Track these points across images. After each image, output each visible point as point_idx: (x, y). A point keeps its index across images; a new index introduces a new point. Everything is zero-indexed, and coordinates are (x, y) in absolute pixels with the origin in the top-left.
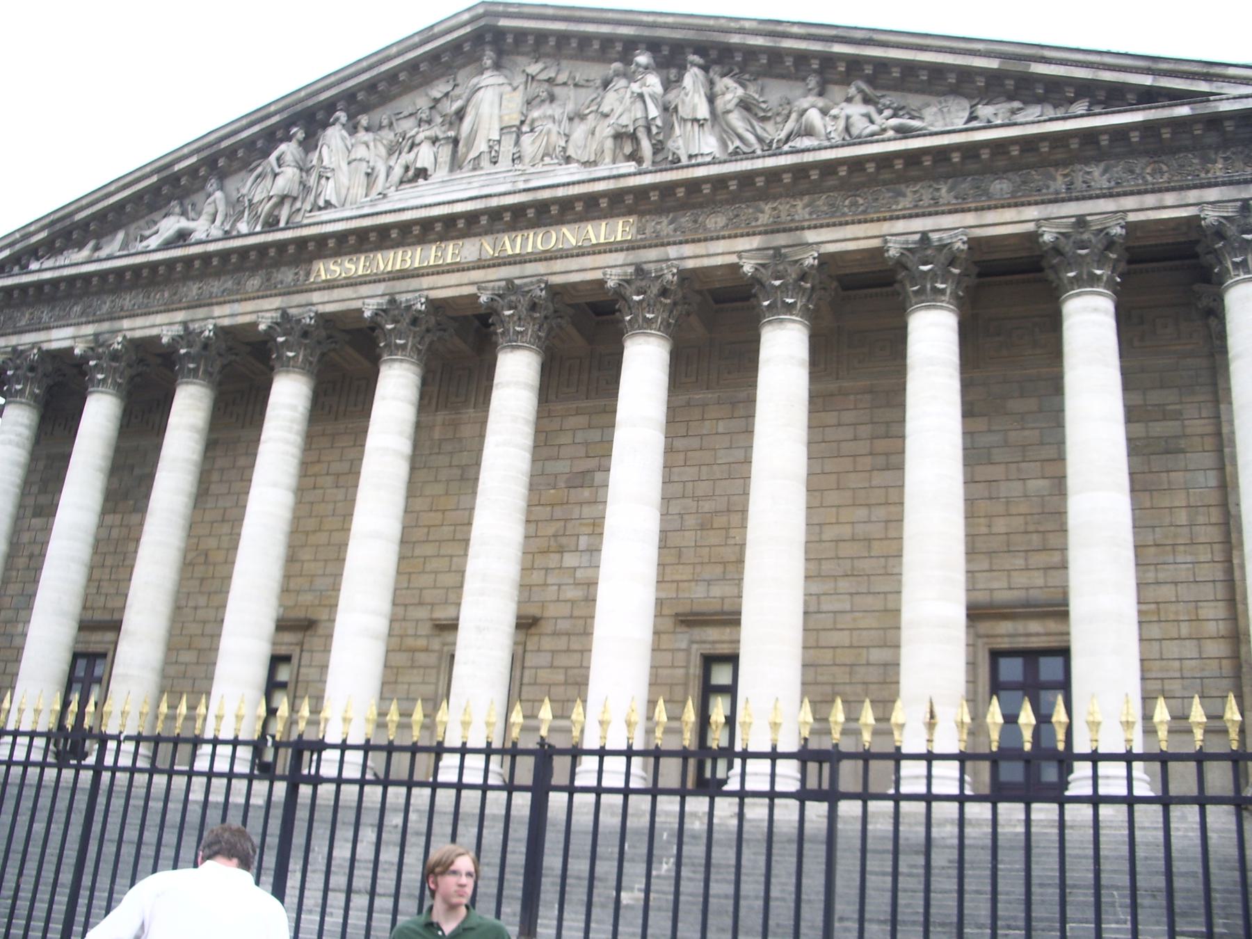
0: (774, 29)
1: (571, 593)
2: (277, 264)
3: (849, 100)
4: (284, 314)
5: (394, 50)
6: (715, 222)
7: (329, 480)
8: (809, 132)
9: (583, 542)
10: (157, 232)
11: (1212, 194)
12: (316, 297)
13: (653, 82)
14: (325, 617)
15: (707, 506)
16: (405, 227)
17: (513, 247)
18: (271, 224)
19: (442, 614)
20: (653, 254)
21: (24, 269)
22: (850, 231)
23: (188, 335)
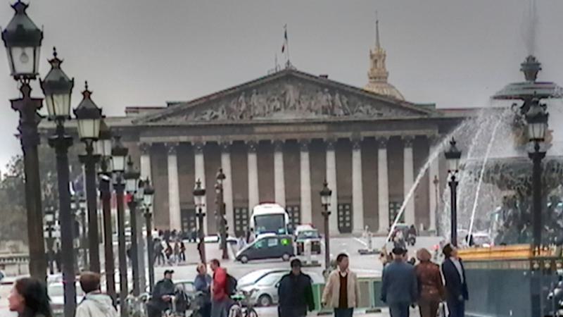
8: (361, 111)
10: (206, 113)
18: (241, 117)
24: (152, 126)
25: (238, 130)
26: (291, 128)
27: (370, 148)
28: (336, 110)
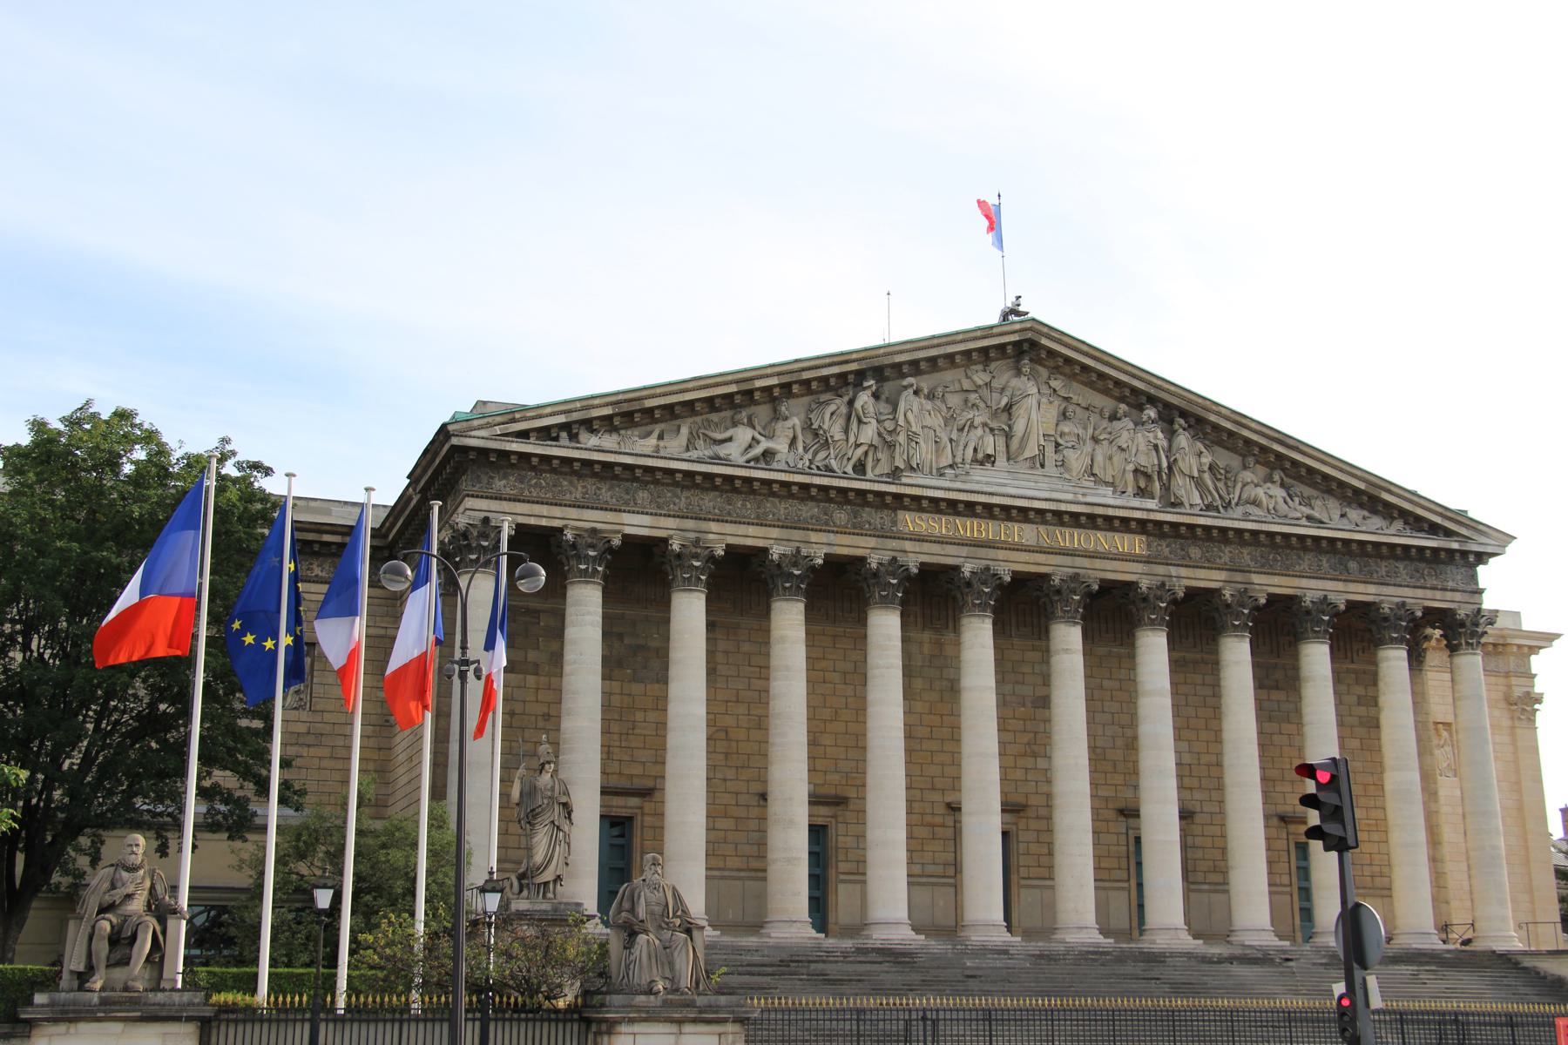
0: (1239, 419)
2: (867, 504)
3: (1269, 479)
4: (894, 559)
5: (961, 337)
6: (1195, 552)
7: (836, 677)
8: (1255, 503)
10: (730, 439)
11: (1458, 596)
12: (908, 545)
13: (1160, 435)
14: (852, 793)
16: (988, 507)
20: (1161, 569)
21: (573, 437)
22: (1276, 580)
23: (796, 558)
25: (841, 516)
27: (1278, 628)
28: (1183, 488)
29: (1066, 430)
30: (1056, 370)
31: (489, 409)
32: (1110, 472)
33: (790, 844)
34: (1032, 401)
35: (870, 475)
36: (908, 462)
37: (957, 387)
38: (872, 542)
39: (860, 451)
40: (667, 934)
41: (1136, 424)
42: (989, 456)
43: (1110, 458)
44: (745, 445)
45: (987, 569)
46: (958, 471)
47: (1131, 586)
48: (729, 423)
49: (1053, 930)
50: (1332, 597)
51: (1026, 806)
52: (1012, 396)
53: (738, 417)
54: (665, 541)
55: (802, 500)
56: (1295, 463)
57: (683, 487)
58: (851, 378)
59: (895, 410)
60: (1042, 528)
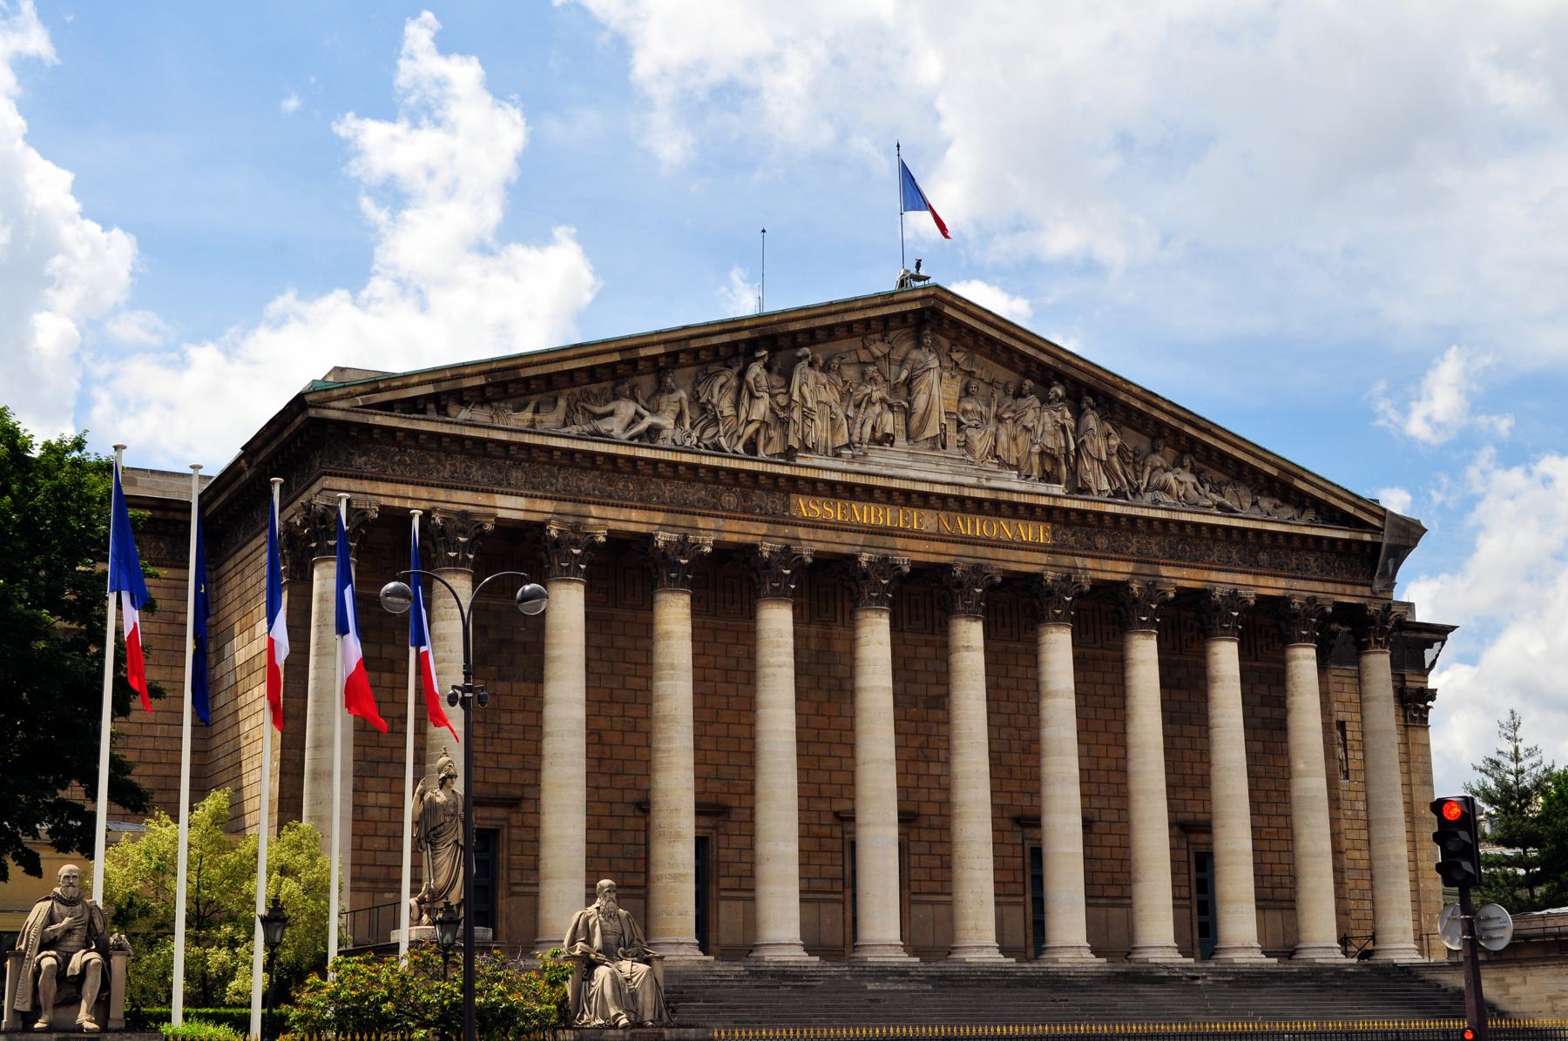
0: (1150, 398)
1: (938, 796)
3: (1178, 463)
4: (788, 547)
5: (860, 304)
6: (1102, 542)
8: (1165, 489)
9: (942, 753)
10: (611, 414)
12: (801, 532)
13: (1068, 415)
15: (1025, 735)
17: (966, 528)
18: (751, 448)
19: (845, 805)
20: (1066, 560)
21: (442, 410)
22: (1185, 573)
23: (683, 546)
24: (392, 431)
25: (729, 499)
26: (925, 520)
27: (1187, 627)
29: (969, 407)
30: (956, 342)
31: (347, 378)
32: (1014, 454)
33: (676, 857)
34: (933, 376)
35: (762, 454)
36: (803, 441)
37: (854, 358)
38: (763, 529)
39: (751, 428)
40: (626, 965)
41: (1042, 403)
42: (888, 435)
43: (1015, 439)
44: (627, 420)
45: (886, 558)
46: (856, 452)
47: (1038, 577)
48: (609, 394)
49: (950, 950)
50: (1241, 592)
51: (918, 815)
52: (913, 370)
53: (619, 389)
54: (541, 526)
55: (689, 482)
56: (1206, 446)
57: (561, 467)
58: (742, 347)
59: (788, 384)
60: (942, 515)
